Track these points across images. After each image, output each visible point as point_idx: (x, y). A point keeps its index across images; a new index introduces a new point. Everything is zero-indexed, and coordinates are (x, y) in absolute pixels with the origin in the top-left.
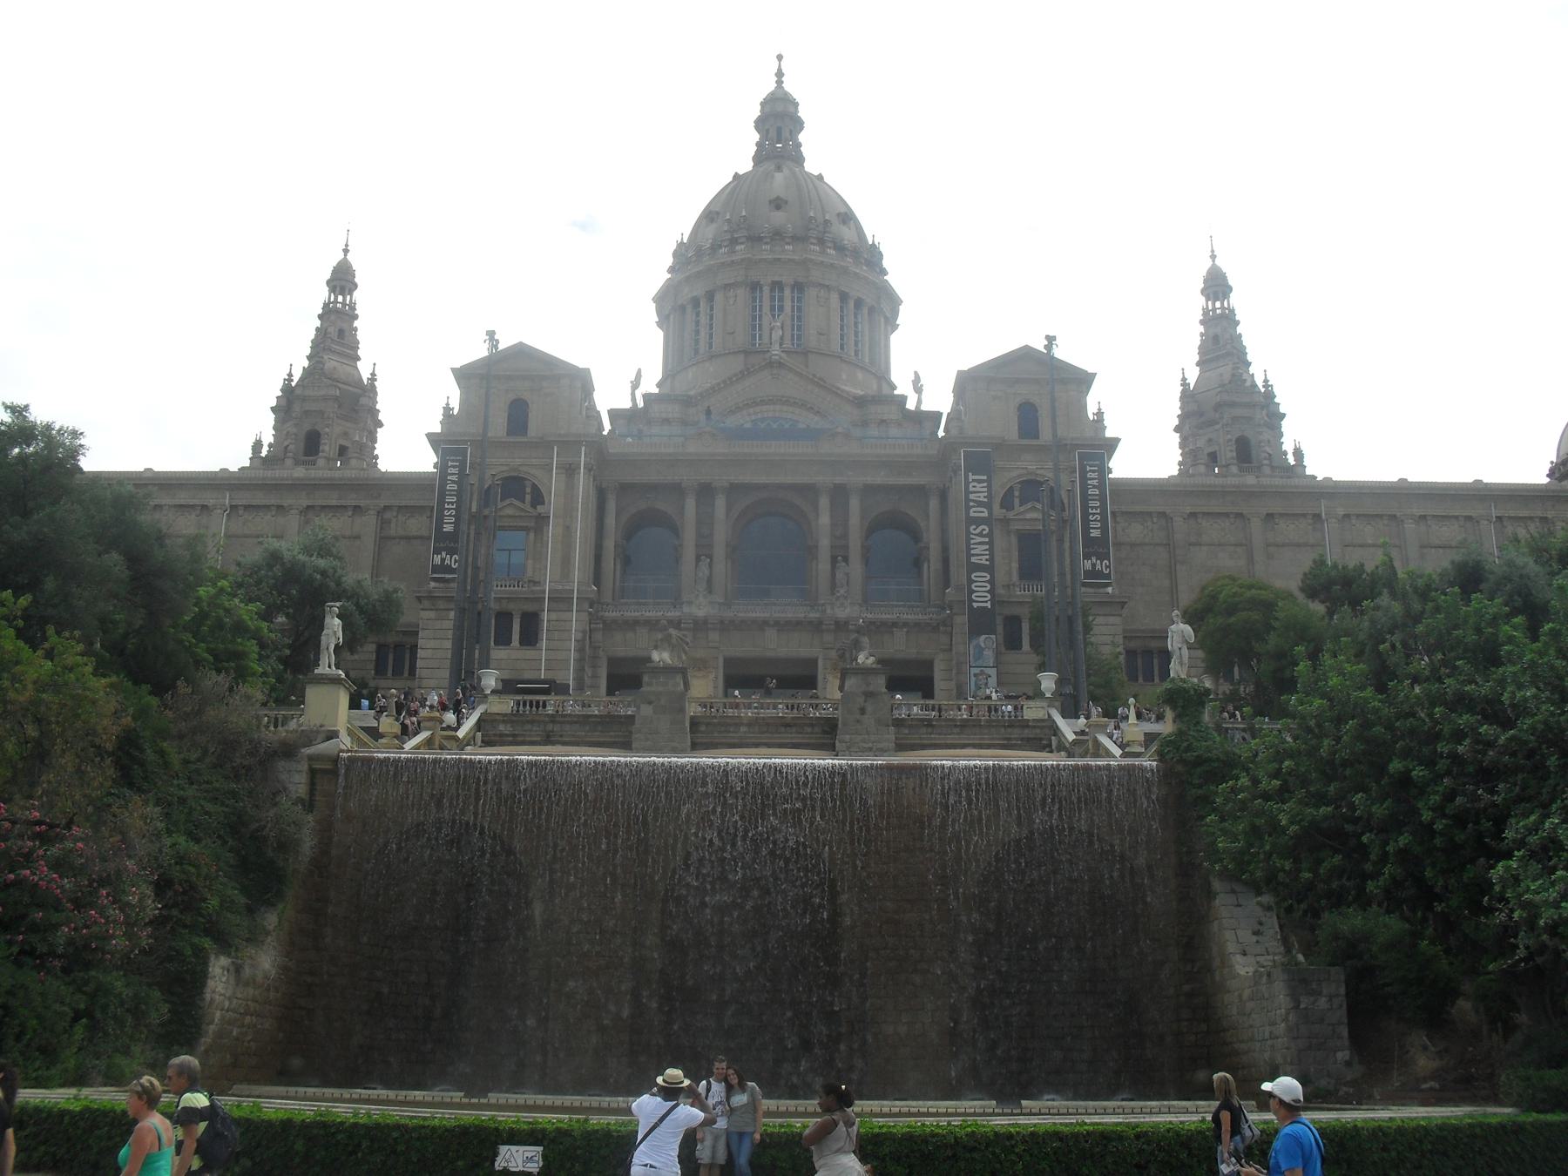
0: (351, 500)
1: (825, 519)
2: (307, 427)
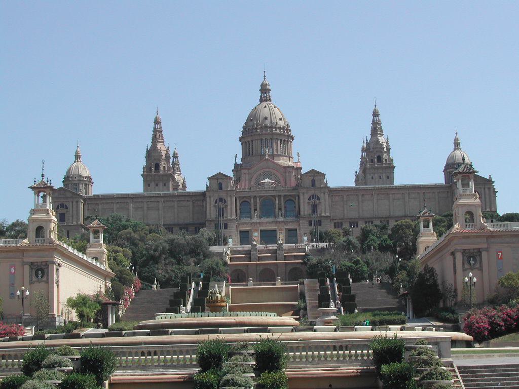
0: (187, 199)
1: (277, 202)
2: (155, 162)
